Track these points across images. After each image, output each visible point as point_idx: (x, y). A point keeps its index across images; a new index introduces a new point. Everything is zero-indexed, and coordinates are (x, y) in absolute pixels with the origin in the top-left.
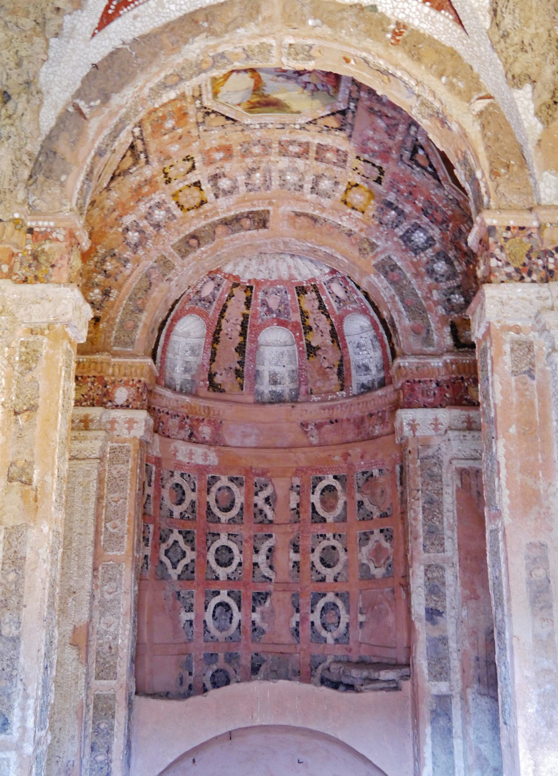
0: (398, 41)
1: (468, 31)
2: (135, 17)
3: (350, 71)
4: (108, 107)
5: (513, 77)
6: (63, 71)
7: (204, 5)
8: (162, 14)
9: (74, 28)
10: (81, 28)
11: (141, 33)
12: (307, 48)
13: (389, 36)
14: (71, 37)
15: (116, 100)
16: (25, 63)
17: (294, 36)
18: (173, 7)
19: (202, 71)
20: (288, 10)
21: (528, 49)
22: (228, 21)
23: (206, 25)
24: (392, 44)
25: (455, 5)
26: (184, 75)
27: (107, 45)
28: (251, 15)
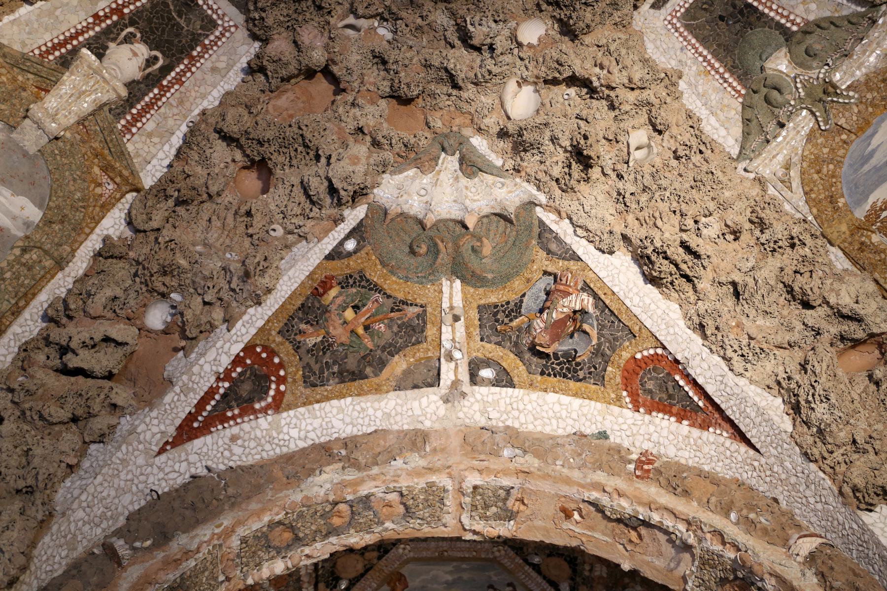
0: (648, 471)
1: (758, 446)
2: (234, 439)
4: (163, 551)
5: (855, 489)
6: (99, 489)
8: (276, 441)
10: (145, 432)
12: (502, 493)
13: (631, 467)
14: (124, 440)
15: (182, 541)
17: (480, 471)
18: (294, 433)
21: (868, 447)
24: (637, 477)
25: (729, 413)
27: (182, 471)
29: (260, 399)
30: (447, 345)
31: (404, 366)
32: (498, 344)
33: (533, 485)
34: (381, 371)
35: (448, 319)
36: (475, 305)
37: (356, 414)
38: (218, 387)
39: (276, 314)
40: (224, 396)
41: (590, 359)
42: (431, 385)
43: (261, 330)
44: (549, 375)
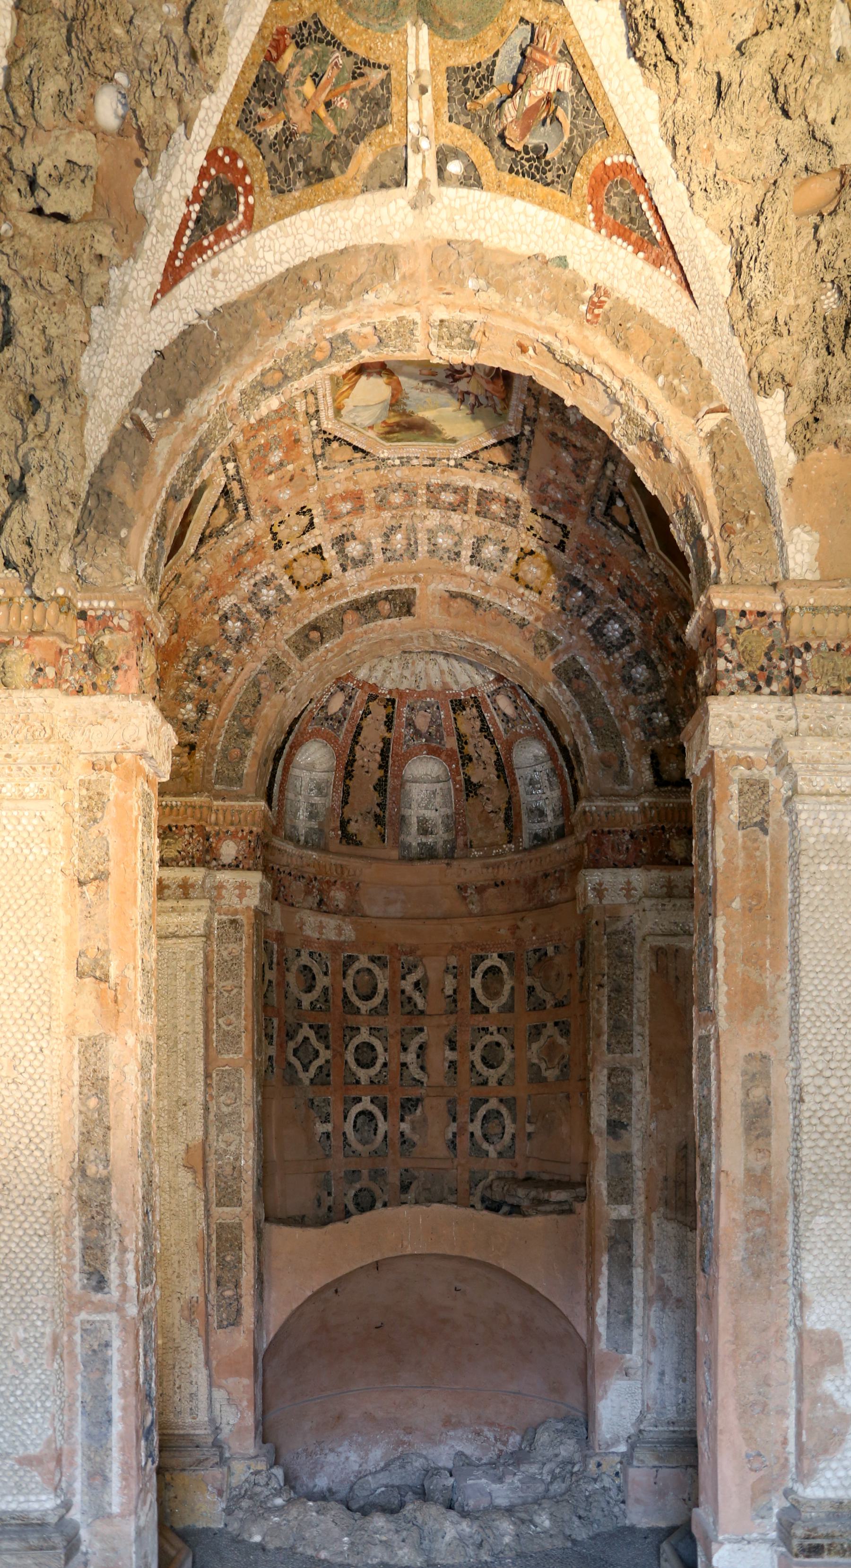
0: (598, 316)
2: (215, 273)
3: (525, 366)
7: (316, 255)
9: (124, 290)
11: (225, 300)
13: (584, 308)
14: (121, 304)
16: (57, 347)
17: (447, 306)
18: (269, 256)
19: (316, 364)
20: (438, 263)
22: (351, 279)
23: (319, 286)
25: (680, 257)
26: (291, 370)
28: (384, 270)
29: (233, 217)
30: (413, 128)
31: (370, 159)
32: (467, 126)
33: (494, 321)
34: (347, 166)
35: (415, 90)
36: (443, 67)
37: (325, 226)
38: (190, 212)
39: (231, 101)
40: (198, 221)
41: (561, 157)
42: (398, 185)
43: (220, 126)
44: (517, 173)
